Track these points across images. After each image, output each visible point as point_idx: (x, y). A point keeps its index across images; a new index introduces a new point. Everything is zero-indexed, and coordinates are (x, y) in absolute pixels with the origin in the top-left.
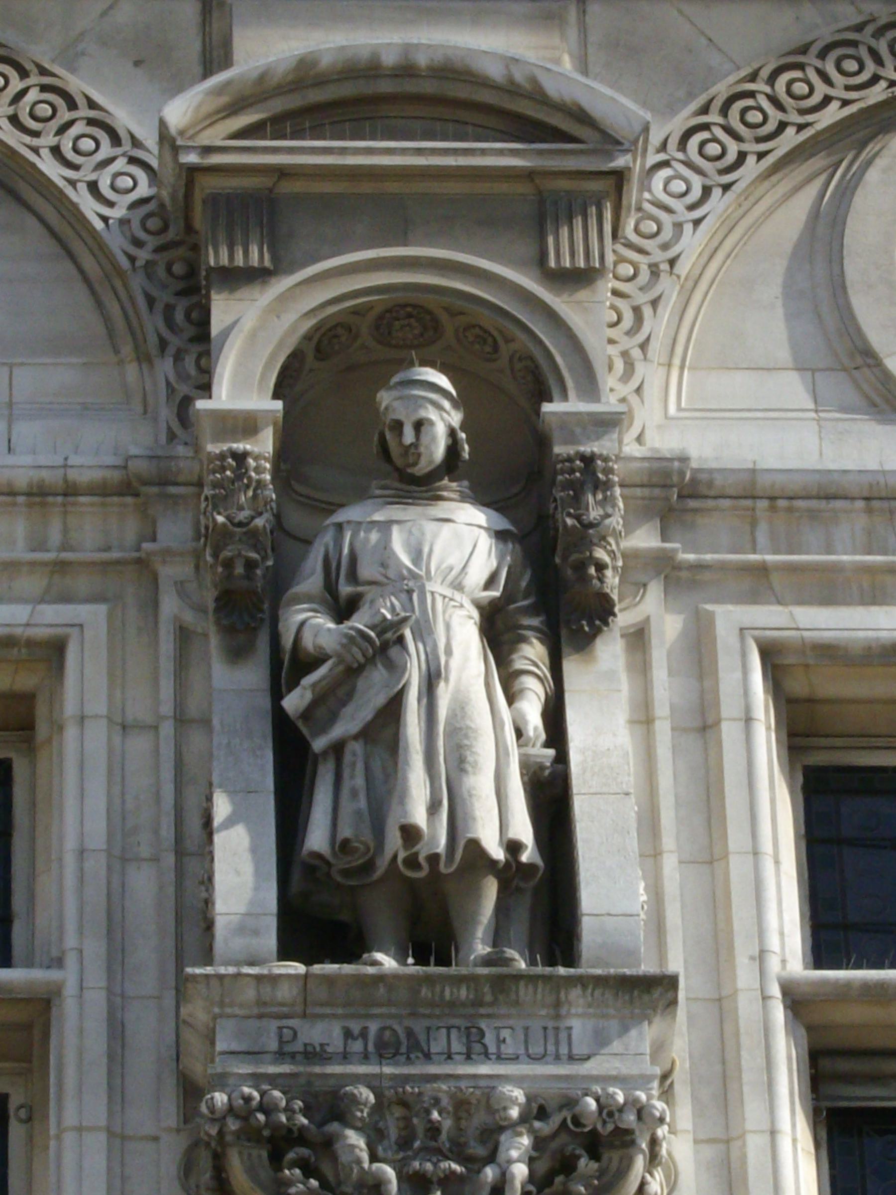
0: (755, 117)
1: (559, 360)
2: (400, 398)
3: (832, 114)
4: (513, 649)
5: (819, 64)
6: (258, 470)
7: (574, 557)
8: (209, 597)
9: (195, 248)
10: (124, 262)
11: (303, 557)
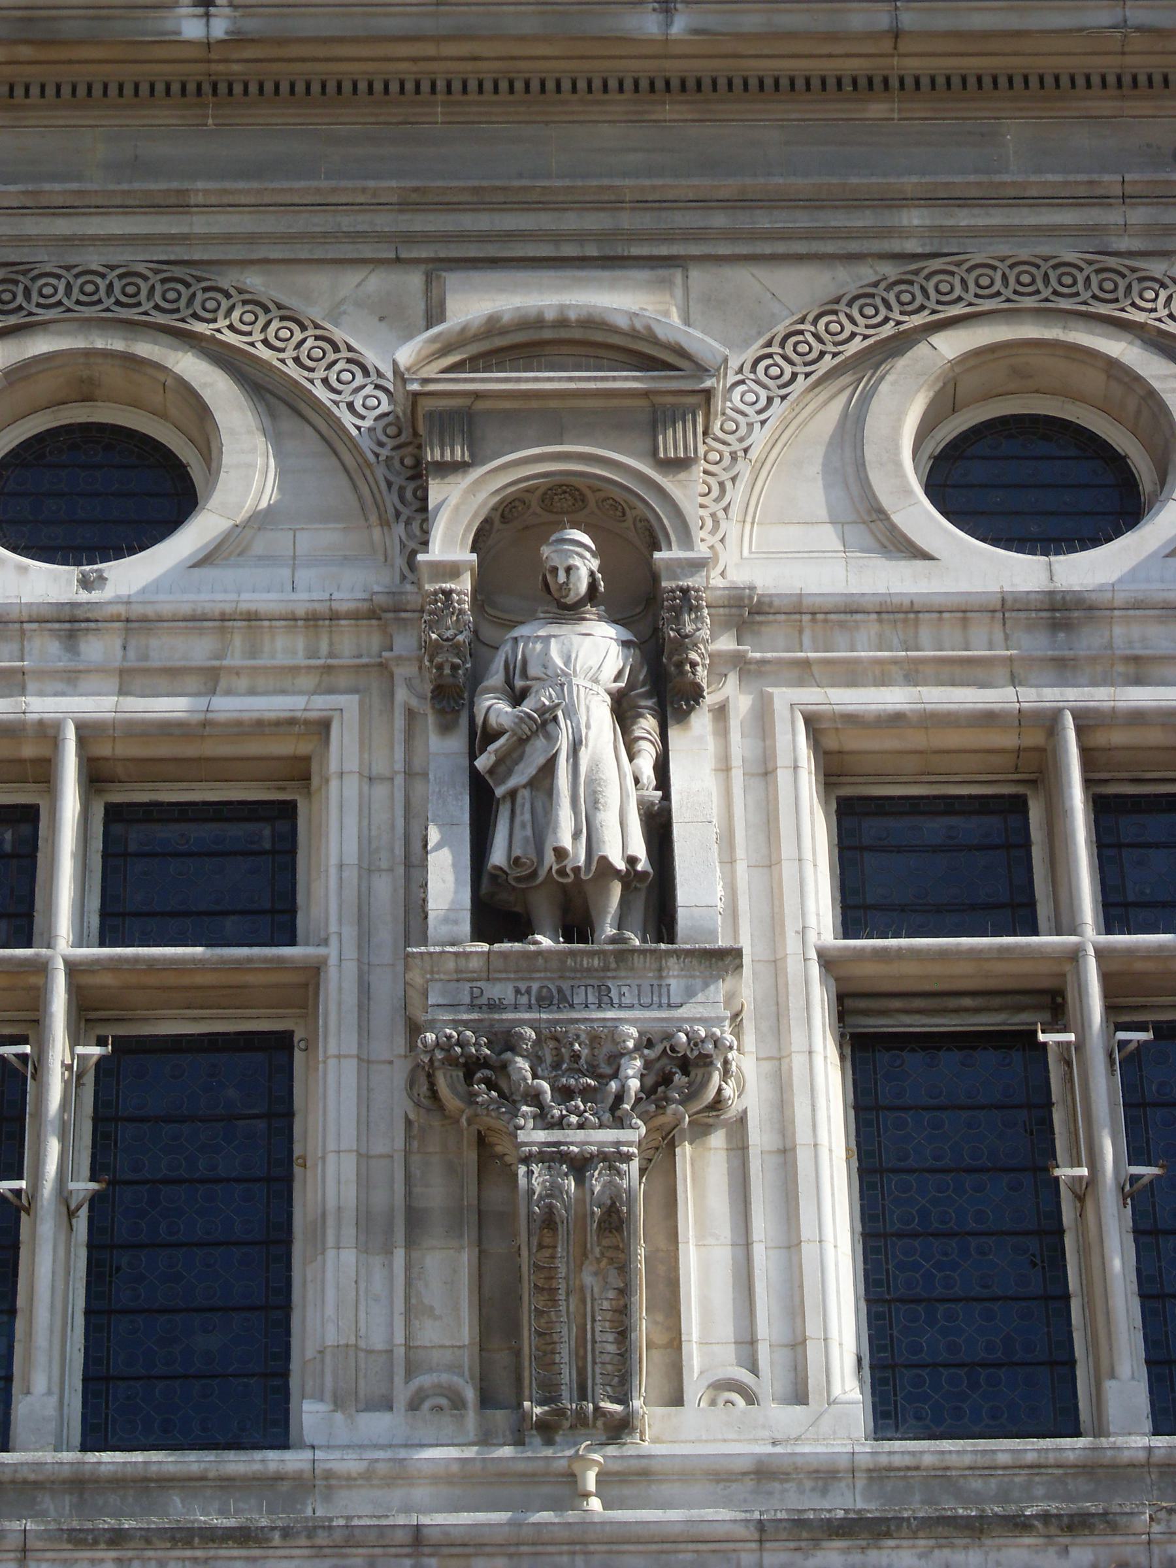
0: (803, 348)
1: (666, 521)
2: (555, 551)
3: (856, 345)
4: (634, 723)
5: (848, 310)
6: (459, 602)
7: (675, 658)
8: (428, 688)
9: (419, 447)
10: (371, 458)
11: (490, 661)
